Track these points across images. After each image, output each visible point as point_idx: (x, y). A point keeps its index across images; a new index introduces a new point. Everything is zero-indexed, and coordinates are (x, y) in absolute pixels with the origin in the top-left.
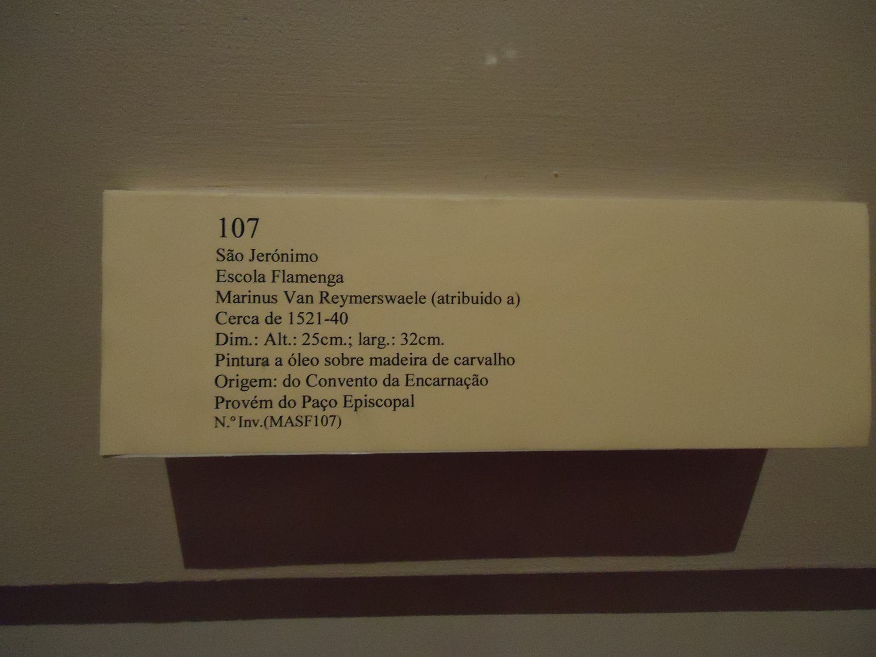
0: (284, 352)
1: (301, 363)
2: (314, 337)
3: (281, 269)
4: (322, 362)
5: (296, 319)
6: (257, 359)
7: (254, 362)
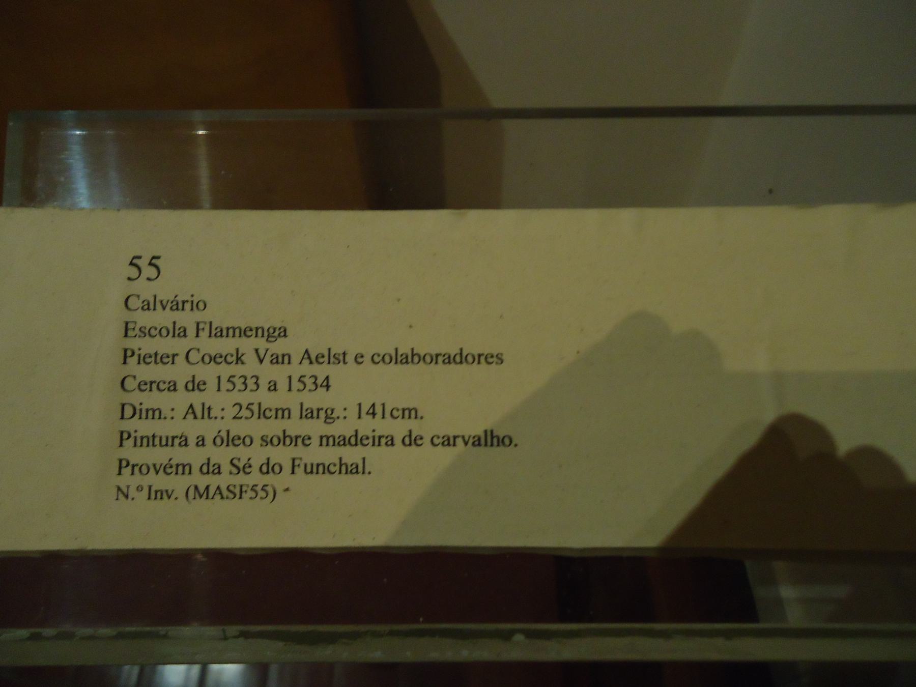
0: (209, 428)
1: (230, 443)
2: (247, 408)
3: (208, 320)
4: (257, 441)
5: (225, 385)
6: (173, 438)
7: (169, 442)
